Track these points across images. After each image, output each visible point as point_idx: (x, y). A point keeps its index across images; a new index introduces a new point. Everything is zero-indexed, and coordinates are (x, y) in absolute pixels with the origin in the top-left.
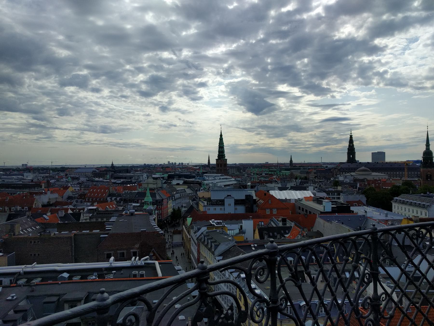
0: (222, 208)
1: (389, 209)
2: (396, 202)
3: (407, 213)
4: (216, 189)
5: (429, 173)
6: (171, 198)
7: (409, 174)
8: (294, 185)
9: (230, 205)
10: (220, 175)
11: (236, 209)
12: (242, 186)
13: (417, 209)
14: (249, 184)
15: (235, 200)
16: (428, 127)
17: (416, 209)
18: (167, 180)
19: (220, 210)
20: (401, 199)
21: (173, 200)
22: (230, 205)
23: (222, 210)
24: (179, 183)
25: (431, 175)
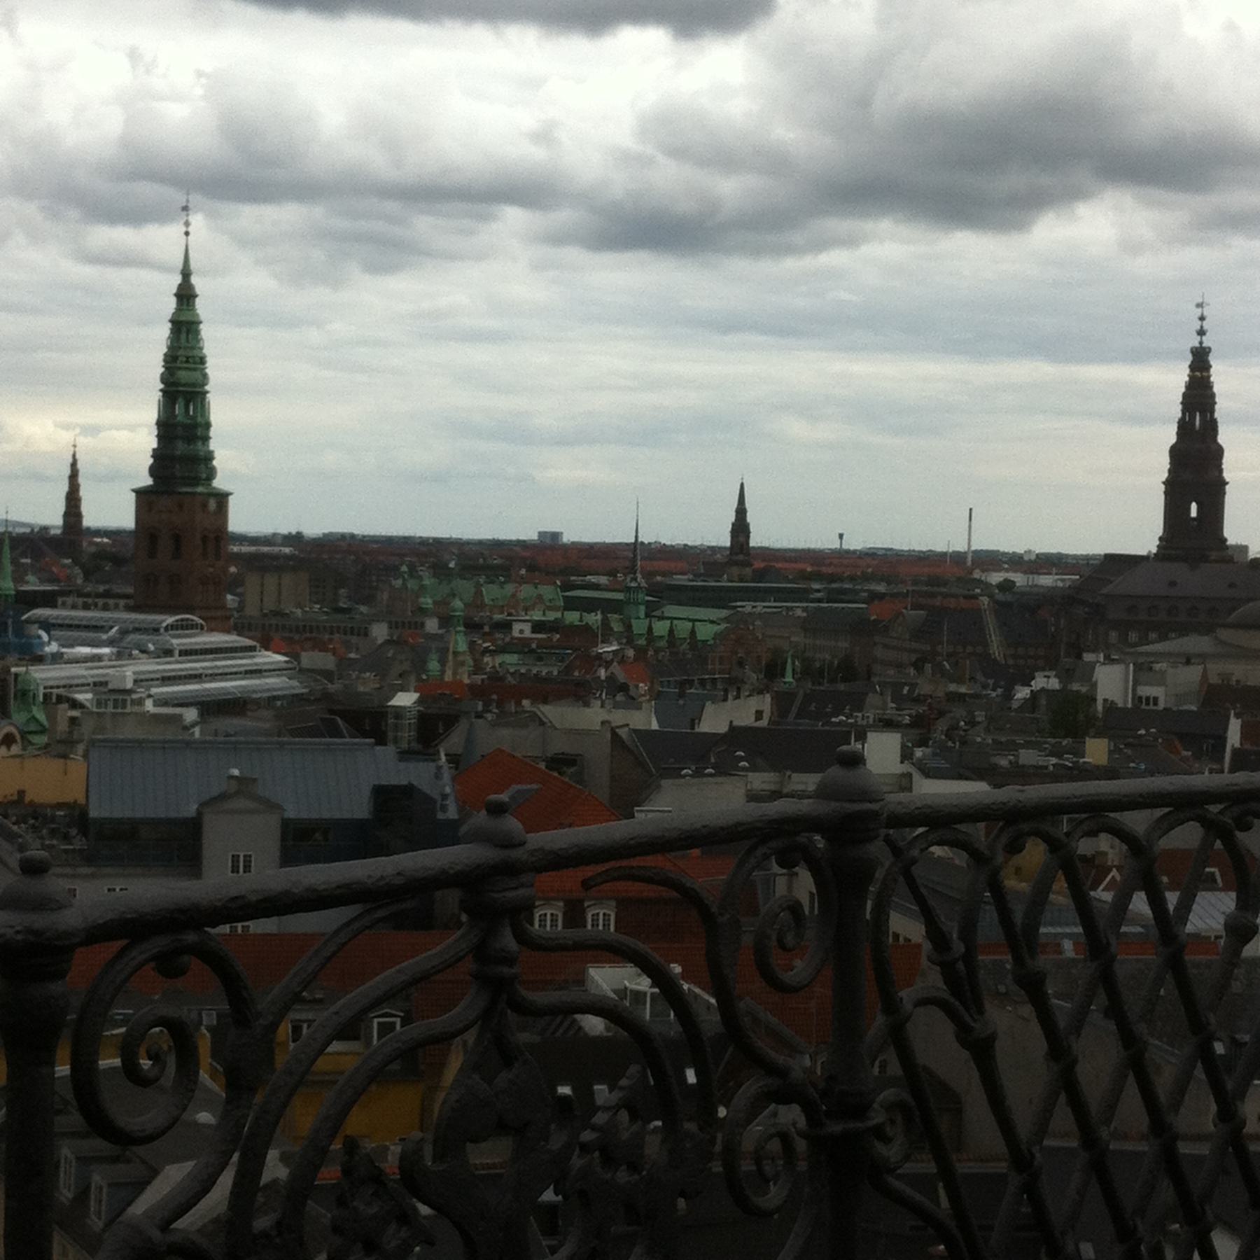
4: (129, 731)
8: (759, 715)
10: (170, 620)
12: (344, 715)
14: (405, 699)
15: (286, 824)
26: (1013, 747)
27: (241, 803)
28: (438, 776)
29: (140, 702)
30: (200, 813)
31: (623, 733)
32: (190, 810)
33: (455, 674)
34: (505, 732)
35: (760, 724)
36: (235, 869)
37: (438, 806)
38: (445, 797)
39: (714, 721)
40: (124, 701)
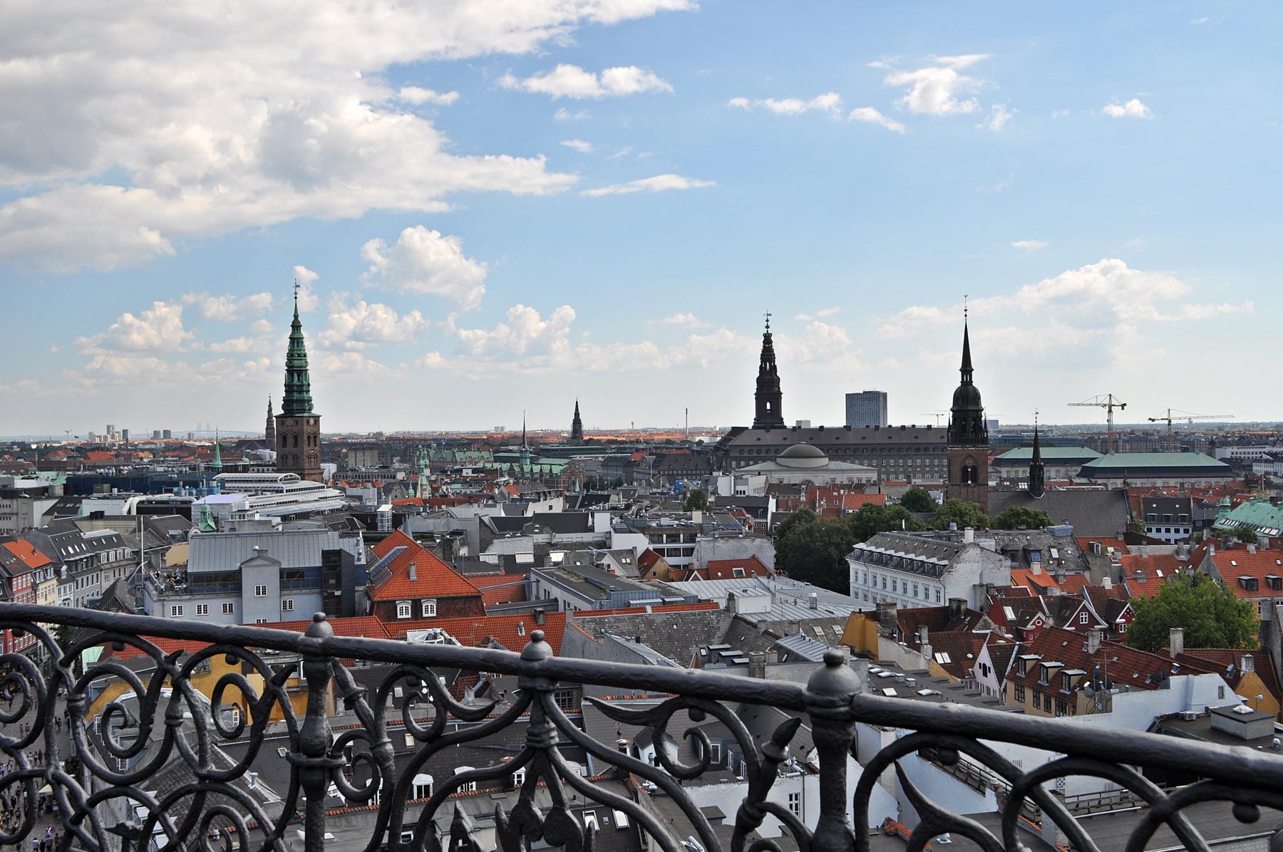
0: (231, 605)
1: (840, 584)
2: (858, 559)
3: (899, 597)
4: (246, 529)
5: (969, 462)
6: (51, 571)
7: (917, 466)
8: (551, 507)
9: (261, 591)
10: (282, 475)
11: (286, 606)
13: (926, 582)
16: (966, 310)
17: (902, 577)
18: (62, 499)
19: (225, 611)
20: (873, 548)
21: (64, 577)
22: (261, 591)
23: (231, 611)
24: (102, 513)
25: (974, 468)
26: (658, 517)
27: (259, 562)
28: (357, 545)
29: (253, 515)
30: (240, 568)
31: (486, 520)
32: (237, 568)
33: (422, 495)
34: (431, 521)
35: (551, 512)
36: (258, 593)
37: (356, 558)
38: (360, 554)
39: (532, 509)
40: (244, 515)
